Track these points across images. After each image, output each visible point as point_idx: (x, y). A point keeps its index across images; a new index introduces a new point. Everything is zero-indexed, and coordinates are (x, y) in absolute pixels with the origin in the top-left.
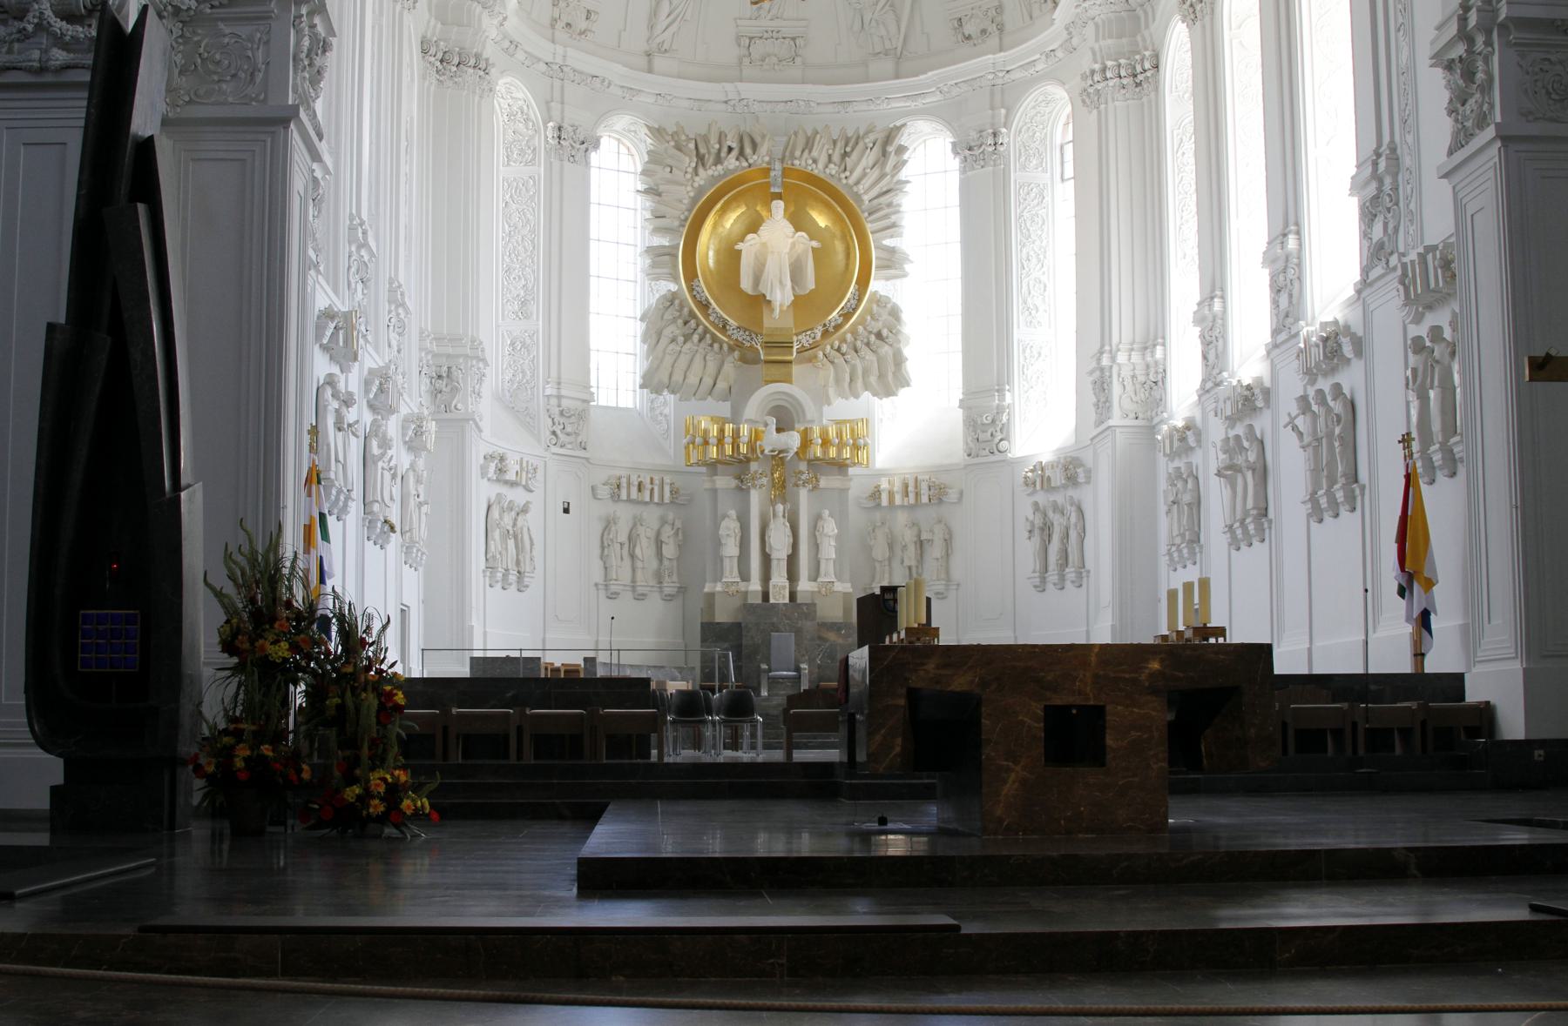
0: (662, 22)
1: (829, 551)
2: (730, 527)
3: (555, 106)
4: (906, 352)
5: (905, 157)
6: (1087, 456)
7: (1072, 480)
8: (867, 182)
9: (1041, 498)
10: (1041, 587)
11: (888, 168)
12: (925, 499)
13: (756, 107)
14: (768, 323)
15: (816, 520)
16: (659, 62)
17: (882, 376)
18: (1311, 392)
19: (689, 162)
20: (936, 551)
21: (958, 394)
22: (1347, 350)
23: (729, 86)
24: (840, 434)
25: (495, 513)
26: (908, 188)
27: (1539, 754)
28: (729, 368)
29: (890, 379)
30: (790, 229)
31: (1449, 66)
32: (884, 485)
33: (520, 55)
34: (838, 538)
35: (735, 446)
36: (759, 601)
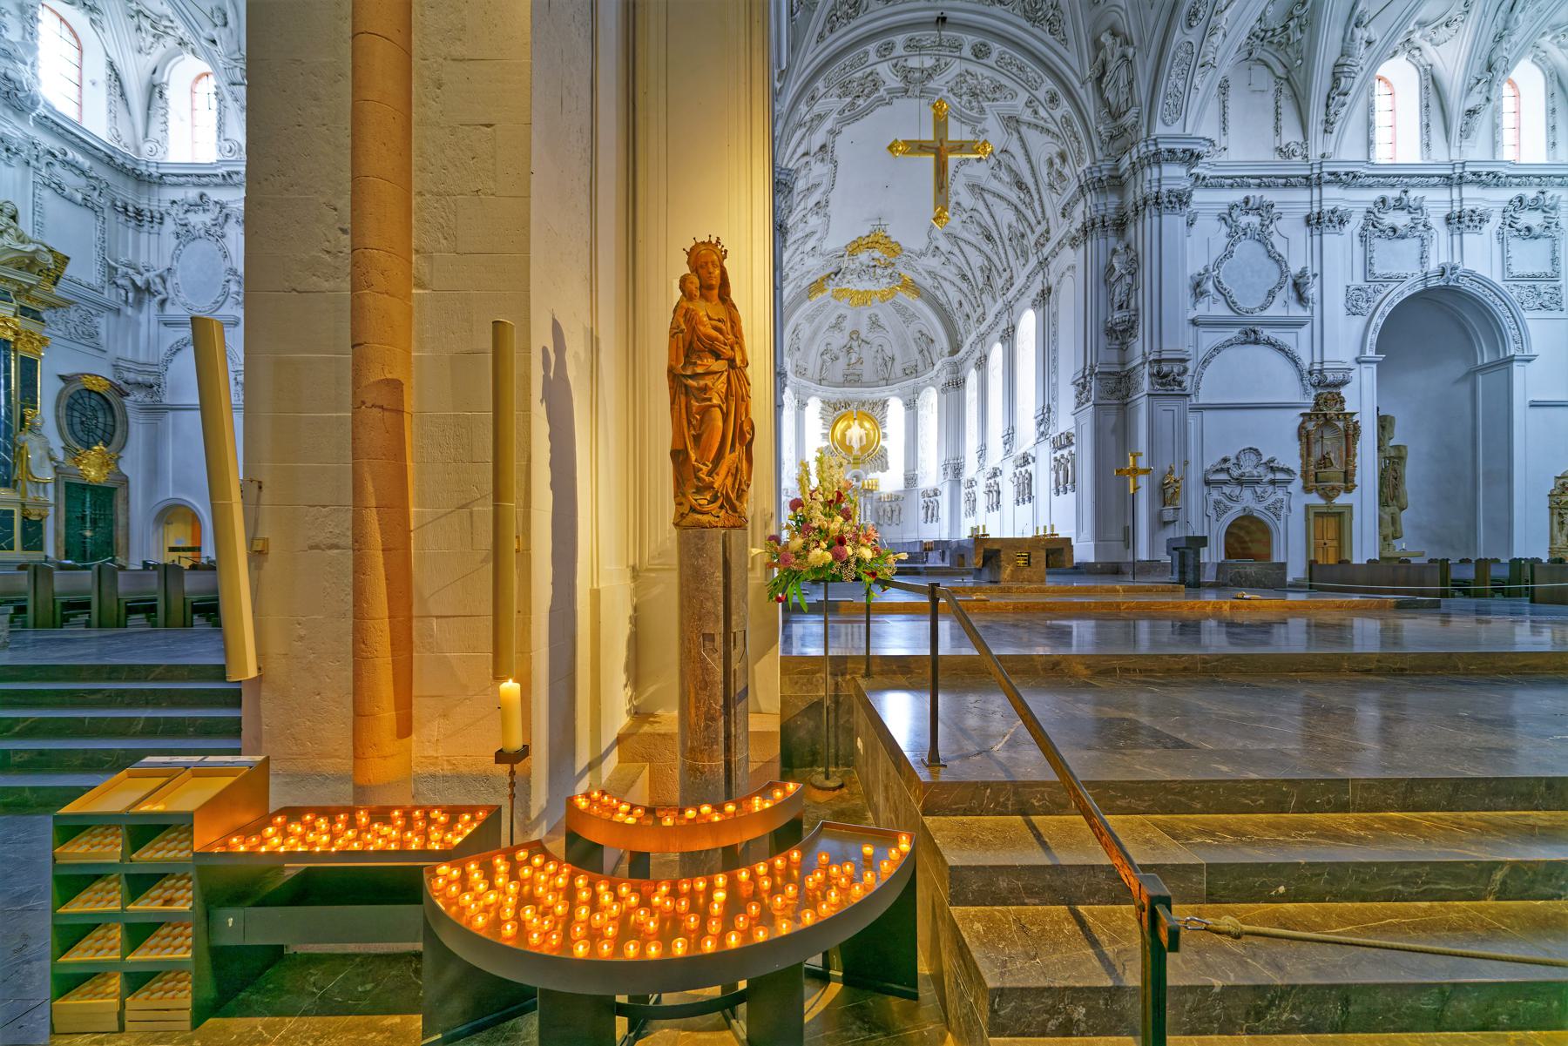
1: (868, 513)
4: (889, 460)
6: (940, 489)
9: (926, 499)
10: (926, 522)
15: (865, 505)
18: (1017, 472)
19: (831, 410)
20: (896, 513)
21: (903, 471)
22: (1030, 460)
27: (1099, 566)
29: (884, 467)
31: (1078, 385)
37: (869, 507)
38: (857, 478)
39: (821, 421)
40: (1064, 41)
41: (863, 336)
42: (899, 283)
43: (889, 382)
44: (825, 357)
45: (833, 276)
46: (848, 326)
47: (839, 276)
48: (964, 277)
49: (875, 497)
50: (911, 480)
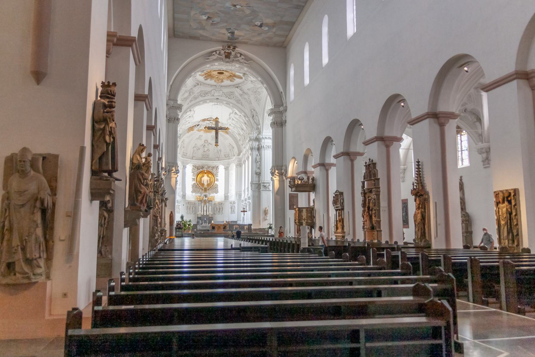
0: (194, 154)
1: (210, 210)
2: (200, 207)
7: (234, 204)
9: (231, 205)
10: (231, 214)
14: (205, 187)
16: (194, 158)
19: (196, 169)
20: (221, 210)
21: (224, 194)
28: (201, 191)
29: (217, 192)
34: (211, 208)
37: (210, 207)
39: (192, 173)
40: (244, 108)
41: (209, 141)
43: (220, 159)
44: (194, 149)
45: (197, 126)
46: (203, 138)
47: (199, 126)
48: (239, 134)
49: (213, 203)
50: (226, 197)
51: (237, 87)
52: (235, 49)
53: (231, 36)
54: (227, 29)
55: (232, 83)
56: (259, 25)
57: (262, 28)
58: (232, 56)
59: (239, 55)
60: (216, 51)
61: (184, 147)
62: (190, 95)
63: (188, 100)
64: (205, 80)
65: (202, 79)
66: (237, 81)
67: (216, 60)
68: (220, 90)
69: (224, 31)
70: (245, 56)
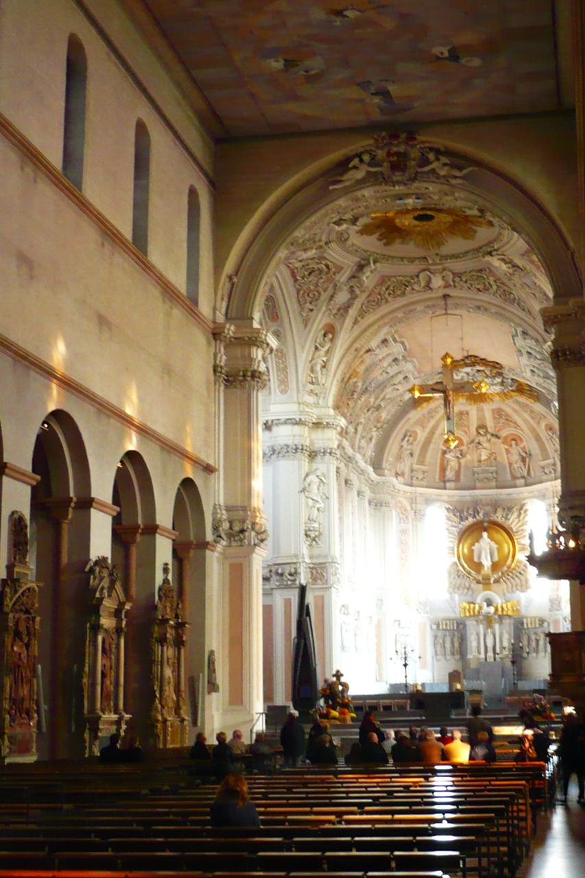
3: (414, 505)
5: (528, 512)
8: (514, 524)
11: (521, 518)
12: (537, 626)
13: (480, 497)
14: (483, 572)
16: (448, 485)
17: (522, 586)
23: (471, 491)
24: (507, 607)
25: (398, 637)
26: (528, 523)
30: (489, 540)
32: (525, 620)
33: (402, 492)
35: (474, 612)
36: (483, 661)
37: (506, 636)
38: (489, 603)
39: (447, 532)
42: (514, 388)
44: (448, 456)
51: (490, 254)
52: (415, 139)
53: (385, 102)
54: (358, 85)
55: (470, 242)
56: (446, 54)
57: (463, 61)
58: (413, 163)
59: (431, 156)
60: (359, 156)
61: (411, 454)
62: (354, 297)
63: (353, 312)
64: (386, 244)
65: (371, 243)
66: (483, 234)
67: (361, 184)
68: (444, 269)
69: (353, 92)
70: (448, 153)
